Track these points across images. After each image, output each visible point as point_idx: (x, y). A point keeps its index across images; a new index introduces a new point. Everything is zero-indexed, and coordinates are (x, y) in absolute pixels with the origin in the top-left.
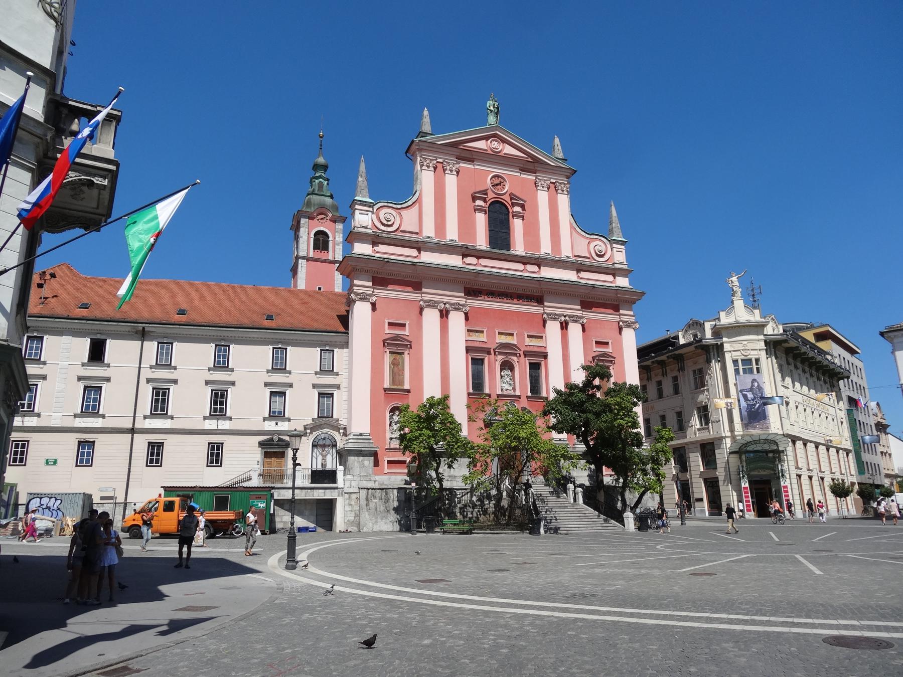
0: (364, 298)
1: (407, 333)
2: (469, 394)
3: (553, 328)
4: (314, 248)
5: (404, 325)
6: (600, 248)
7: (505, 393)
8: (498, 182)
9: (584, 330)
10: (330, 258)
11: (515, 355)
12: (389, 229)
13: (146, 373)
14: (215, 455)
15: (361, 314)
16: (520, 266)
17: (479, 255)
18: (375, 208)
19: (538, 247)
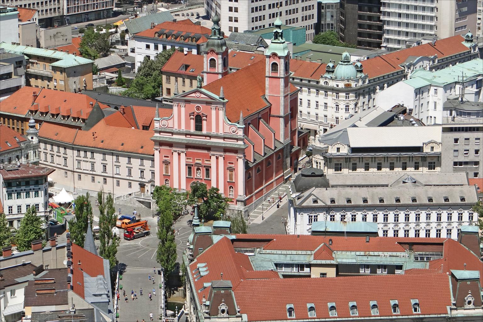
0: (157, 150)
1: (169, 159)
2: (187, 177)
3: (213, 159)
4: (210, 66)
5: (168, 157)
6: (233, 129)
7: (197, 177)
8: (198, 108)
9: (224, 159)
10: (217, 72)
11: (200, 166)
12: (165, 127)
13: (115, 164)
14: (130, 186)
15: (157, 153)
16: (204, 138)
17: (191, 135)
18: (160, 121)
19: (211, 130)
